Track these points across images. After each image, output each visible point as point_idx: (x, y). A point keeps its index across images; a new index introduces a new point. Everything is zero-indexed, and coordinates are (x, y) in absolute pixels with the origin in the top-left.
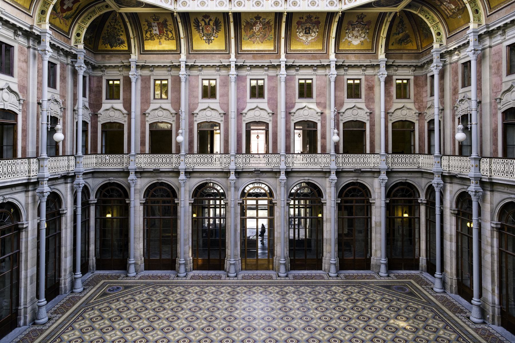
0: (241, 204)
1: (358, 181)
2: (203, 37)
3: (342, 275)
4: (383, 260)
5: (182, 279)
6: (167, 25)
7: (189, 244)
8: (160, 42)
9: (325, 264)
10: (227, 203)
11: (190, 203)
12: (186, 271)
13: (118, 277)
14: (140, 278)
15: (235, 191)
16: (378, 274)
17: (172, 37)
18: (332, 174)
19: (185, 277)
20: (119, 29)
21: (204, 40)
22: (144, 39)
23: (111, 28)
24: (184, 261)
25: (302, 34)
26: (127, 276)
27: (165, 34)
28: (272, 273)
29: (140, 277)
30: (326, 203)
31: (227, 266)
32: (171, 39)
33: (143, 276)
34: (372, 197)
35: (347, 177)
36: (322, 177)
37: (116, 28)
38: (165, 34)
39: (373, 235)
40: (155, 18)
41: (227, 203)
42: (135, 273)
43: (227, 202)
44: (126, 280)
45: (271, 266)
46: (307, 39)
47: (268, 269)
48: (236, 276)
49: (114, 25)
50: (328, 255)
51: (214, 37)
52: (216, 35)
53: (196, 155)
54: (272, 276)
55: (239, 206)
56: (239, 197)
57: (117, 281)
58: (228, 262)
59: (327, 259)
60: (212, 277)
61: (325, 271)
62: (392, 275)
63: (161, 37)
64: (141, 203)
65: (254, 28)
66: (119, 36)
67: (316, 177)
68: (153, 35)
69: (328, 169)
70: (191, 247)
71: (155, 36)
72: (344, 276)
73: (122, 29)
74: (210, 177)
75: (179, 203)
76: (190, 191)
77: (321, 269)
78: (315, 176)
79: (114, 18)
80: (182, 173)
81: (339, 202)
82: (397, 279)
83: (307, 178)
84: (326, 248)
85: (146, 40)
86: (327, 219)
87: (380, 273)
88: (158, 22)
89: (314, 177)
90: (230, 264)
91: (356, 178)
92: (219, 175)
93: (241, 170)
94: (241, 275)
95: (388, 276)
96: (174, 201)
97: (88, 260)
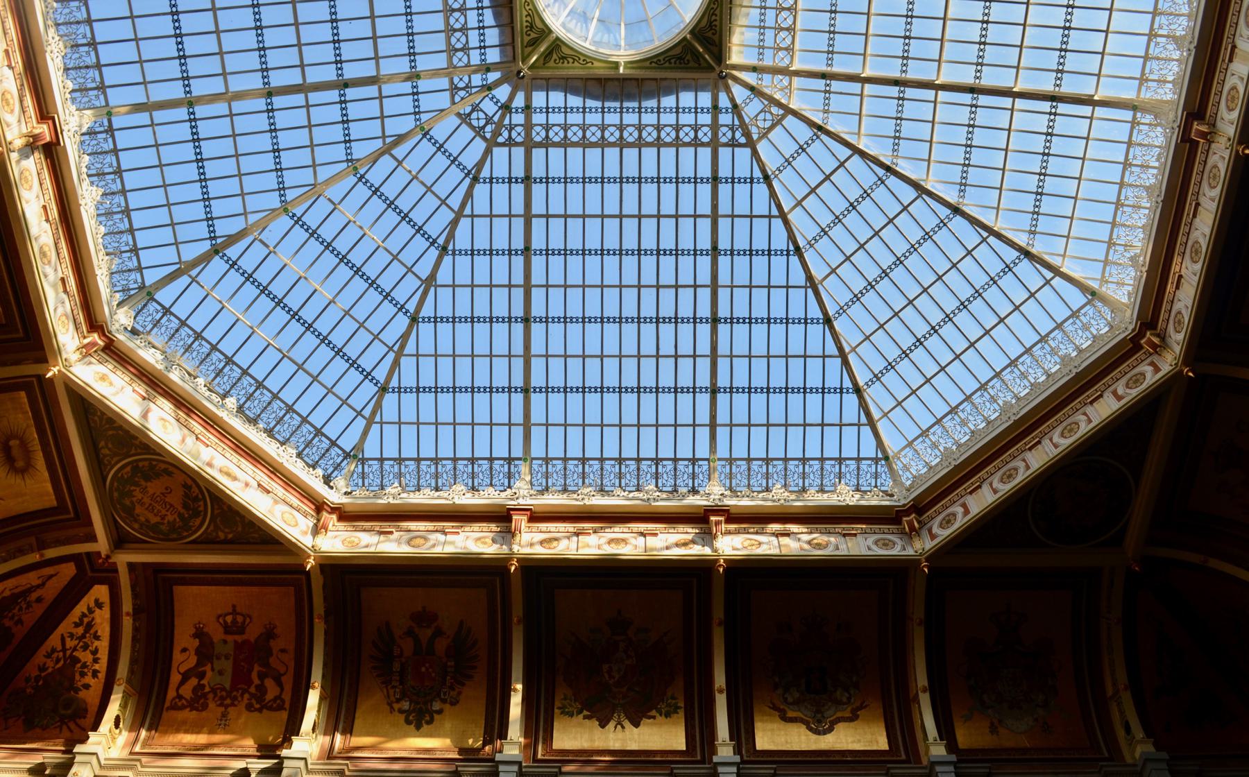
2: (398, 701)
6: (269, 652)
8: (224, 715)
17: (276, 699)
20: (85, 666)
21: (401, 711)
22: (167, 704)
23: (58, 660)
25: (797, 695)
27: (253, 690)
32: (271, 709)
37: (78, 660)
38: (253, 690)
40: (234, 621)
46: (818, 711)
49: (75, 649)
51: (444, 701)
52: (453, 693)
63: (235, 698)
65: (605, 667)
66: (77, 690)
68: (207, 689)
71: (211, 696)
73: (97, 667)
79: (86, 620)
85: (174, 707)
88: (239, 638)
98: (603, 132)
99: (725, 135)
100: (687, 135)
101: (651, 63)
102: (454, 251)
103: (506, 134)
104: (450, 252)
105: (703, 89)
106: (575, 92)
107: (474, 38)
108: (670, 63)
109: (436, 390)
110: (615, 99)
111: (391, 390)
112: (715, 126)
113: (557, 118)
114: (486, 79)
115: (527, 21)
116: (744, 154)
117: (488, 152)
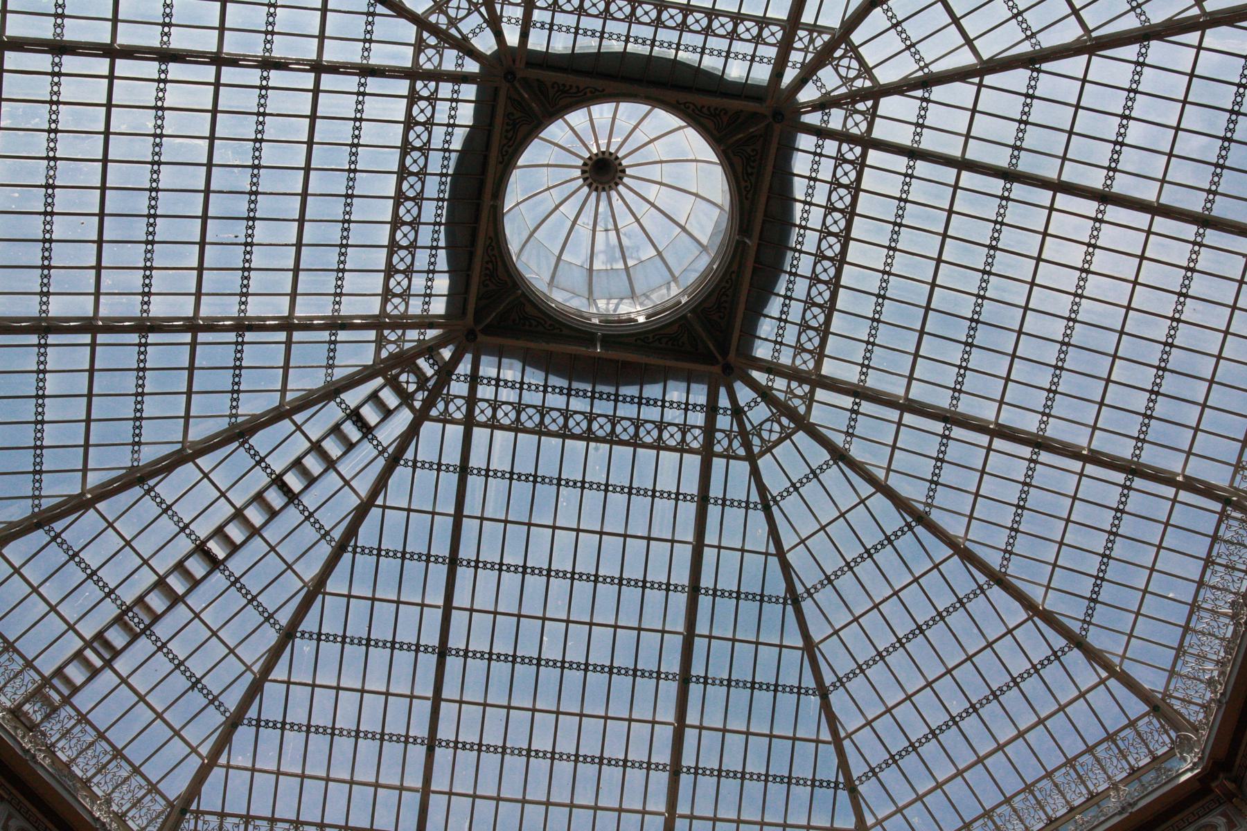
98: (820, 281)
99: (857, 126)
100: (848, 174)
101: (747, 199)
102: (927, 504)
103: (797, 402)
104: (927, 509)
105: (794, 140)
106: (764, 302)
107: (674, 415)
108: (752, 174)
109: (1100, 579)
110: (783, 257)
111: (1084, 633)
112: (843, 137)
113: (791, 335)
114: (725, 409)
115: (667, 343)
116: (888, 105)
117: (813, 433)
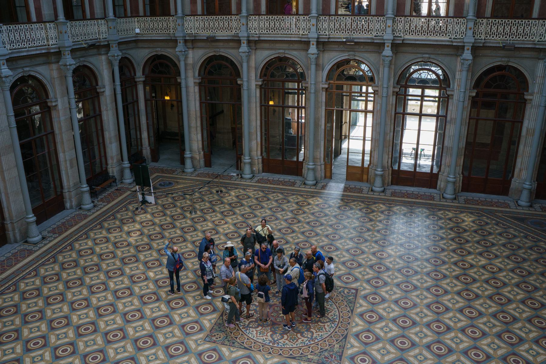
0: (327, 89)
1: (510, 64)
3: (462, 199)
4: (528, 183)
5: (245, 182)
7: (257, 139)
9: (441, 181)
10: (307, 87)
11: (256, 85)
12: (252, 172)
13: (174, 171)
14: (198, 176)
15: (317, 70)
16: (517, 202)
18: (466, 51)
19: (251, 179)
24: (250, 160)
26: (183, 172)
28: (365, 186)
29: (198, 174)
30: (452, 95)
31: (304, 171)
33: (201, 173)
34: (530, 91)
35: (492, 56)
36: (452, 55)
39: (521, 147)
41: (307, 87)
42: (193, 169)
43: (307, 85)
44: (181, 175)
45: (365, 177)
47: (361, 180)
48: (315, 185)
50: (447, 169)
53: (263, 17)
54: (363, 189)
55: (324, 93)
56: (324, 80)
57: (171, 176)
58: (306, 166)
59: (445, 174)
60: (284, 183)
61: (440, 190)
62: (537, 206)
64: (195, 83)
67: (442, 54)
69: (460, 42)
70: (259, 143)
72: (464, 199)
74: (285, 49)
75: (242, 84)
76: (256, 69)
77: (435, 188)
78: (439, 52)
80: (244, 43)
81: (474, 94)
82: (543, 212)
83: (427, 56)
84: (446, 160)
86: (451, 119)
87: (519, 202)
89: (439, 54)
90: (308, 169)
91: (506, 59)
92: (296, 46)
93: (327, 40)
94: (322, 184)
95: (531, 206)
96: (237, 82)
97: (142, 150)
